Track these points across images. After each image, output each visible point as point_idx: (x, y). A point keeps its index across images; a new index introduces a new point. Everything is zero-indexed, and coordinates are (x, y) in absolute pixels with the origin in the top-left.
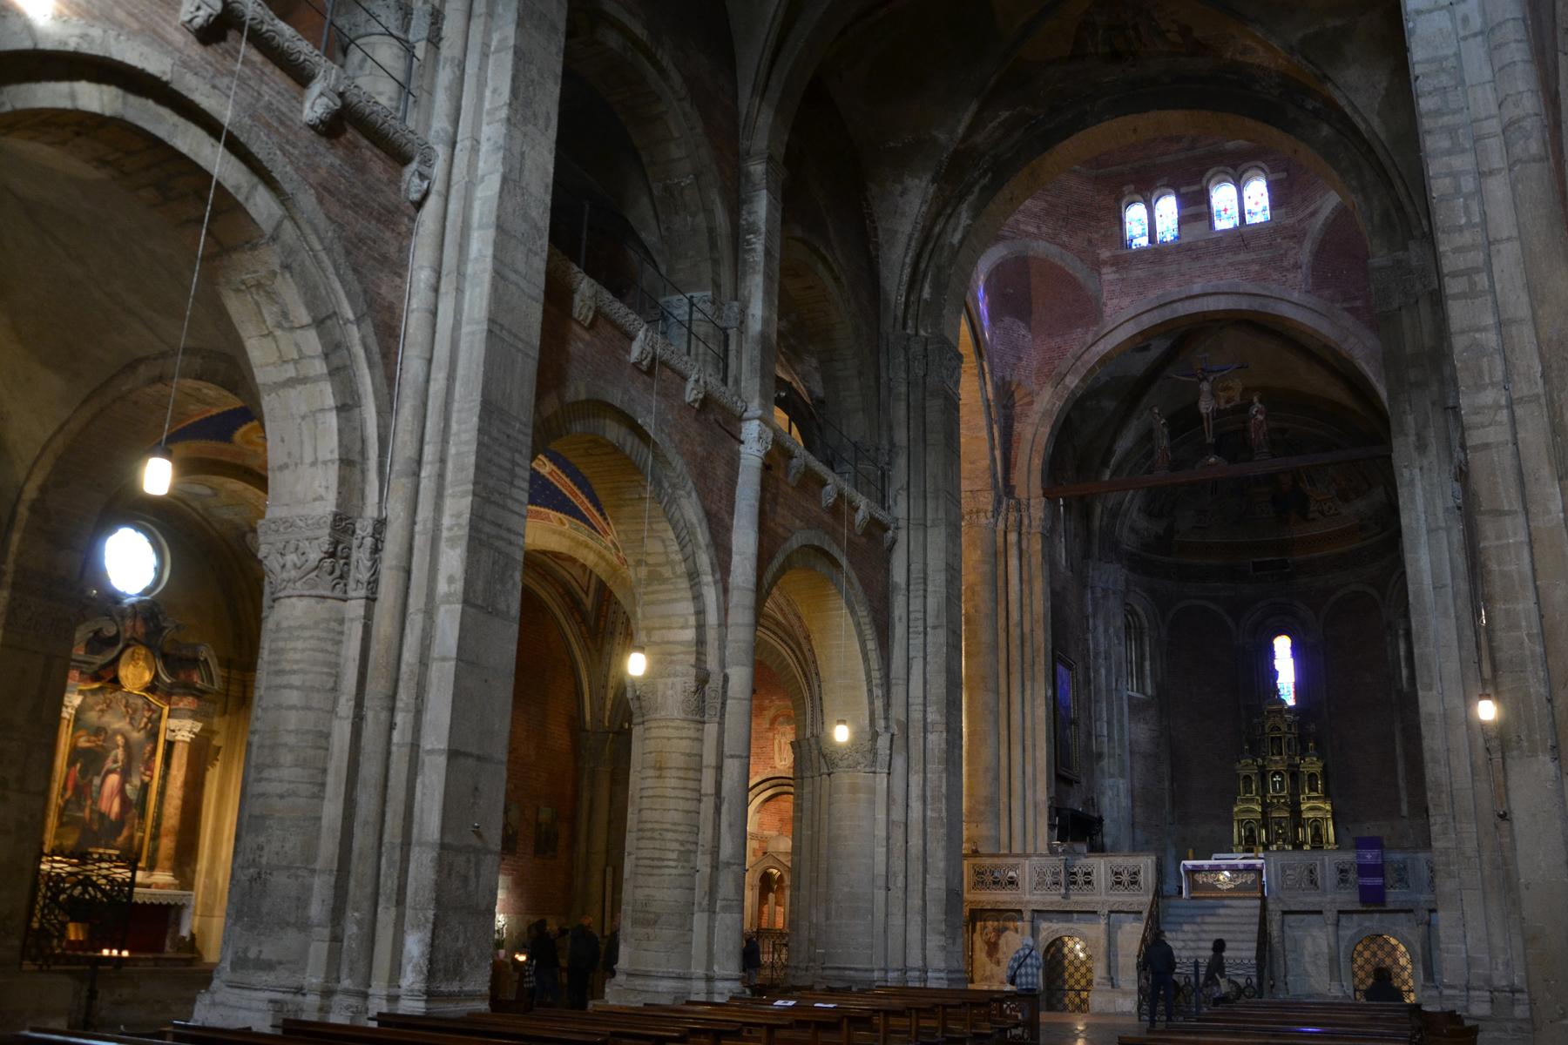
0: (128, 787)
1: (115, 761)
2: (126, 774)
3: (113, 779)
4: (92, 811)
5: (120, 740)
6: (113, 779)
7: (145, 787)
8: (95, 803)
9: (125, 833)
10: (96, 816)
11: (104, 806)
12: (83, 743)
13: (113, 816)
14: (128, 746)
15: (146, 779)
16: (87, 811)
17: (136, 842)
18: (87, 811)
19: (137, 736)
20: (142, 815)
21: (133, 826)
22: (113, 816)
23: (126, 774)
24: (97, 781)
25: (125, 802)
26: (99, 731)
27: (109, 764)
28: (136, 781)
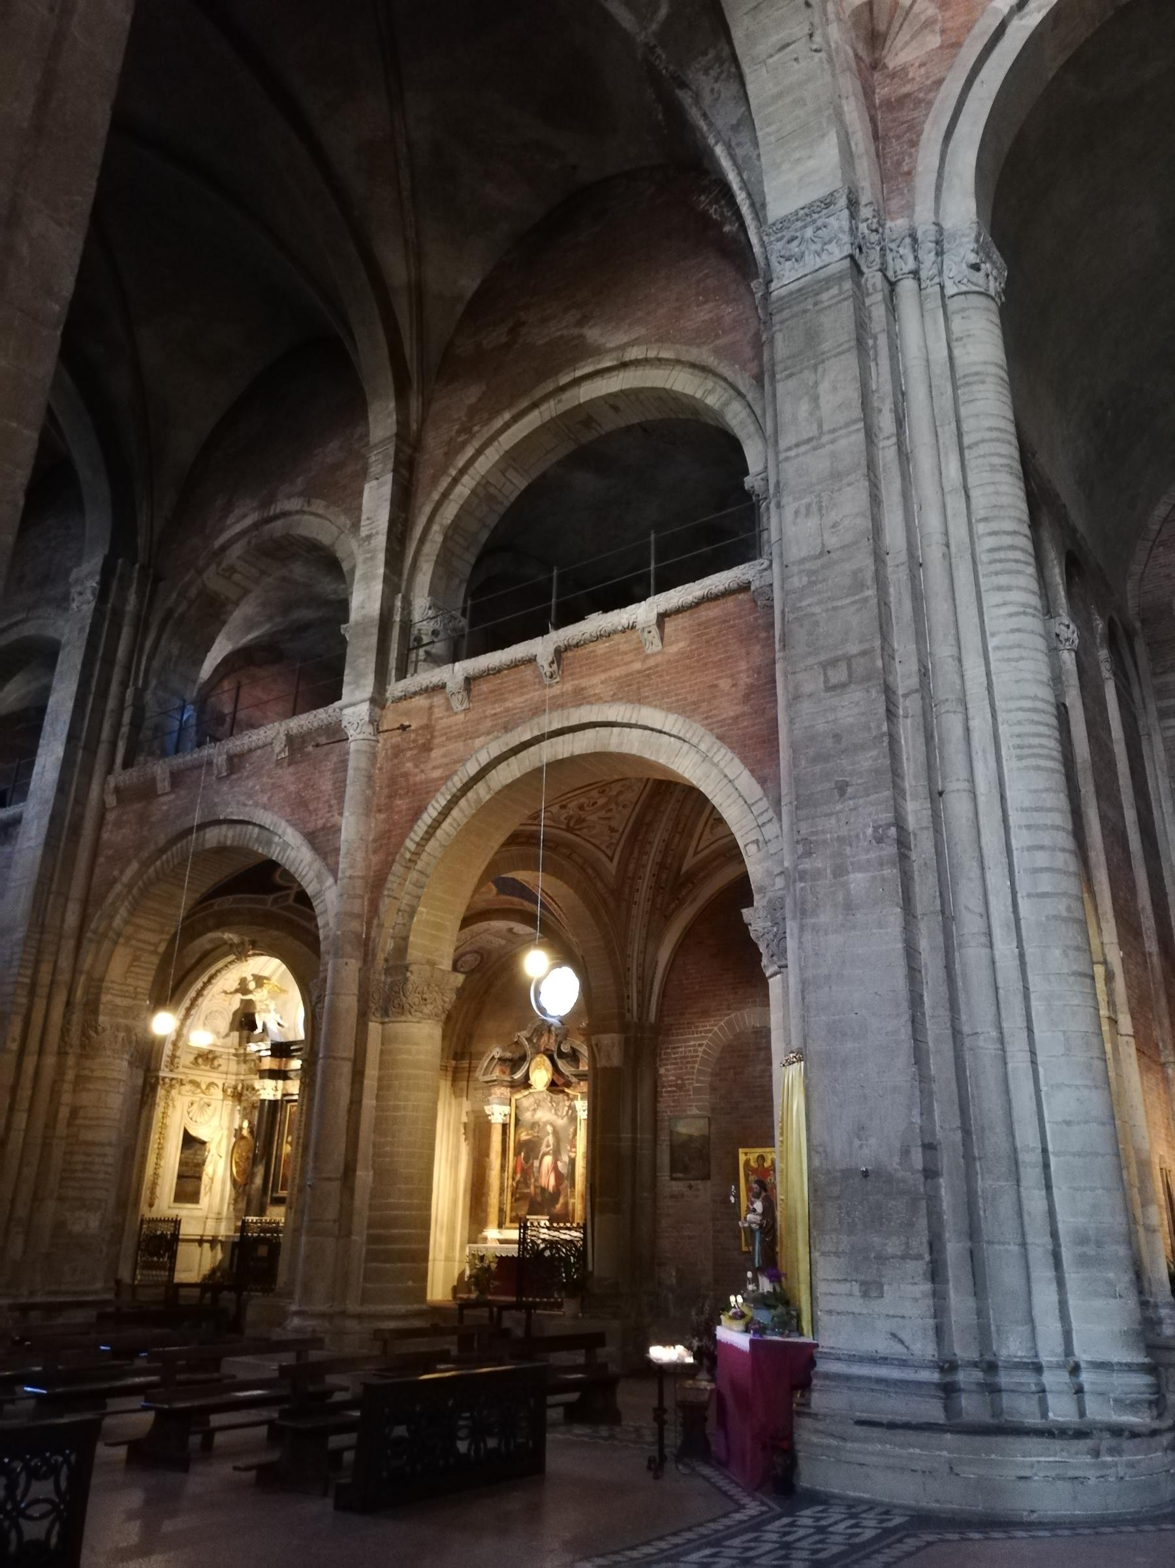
0: (559, 1164)
1: (548, 1146)
2: (556, 1154)
3: (548, 1160)
4: (536, 1187)
5: (549, 1129)
6: (548, 1160)
7: (572, 1162)
8: (536, 1180)
9: (561, 1200)
10: (538, 1191)
11: (543, 1182)
12: (524, 1137)
13: (551, 1189)
14: (555, 1133)
15: (572, 1155)
16: (532, 1188)
17: (570, 1207)
18: (532, 1188)
19: (561, 1122)
20: (573, 1185)
21: (566, 1195)
22: (551, 1189)
23: (556, 1154)
24: (536, 1163)
25: (559, 1177)
26: (534, 1125)
27: (544, 1149)
28: (565, 1158)
